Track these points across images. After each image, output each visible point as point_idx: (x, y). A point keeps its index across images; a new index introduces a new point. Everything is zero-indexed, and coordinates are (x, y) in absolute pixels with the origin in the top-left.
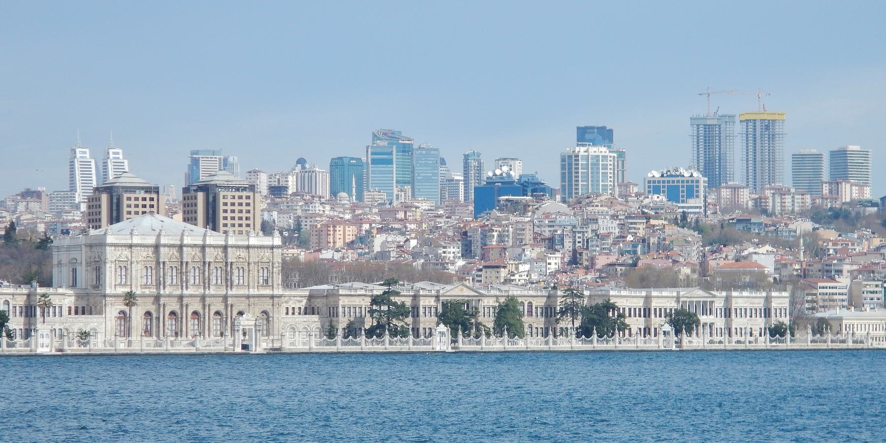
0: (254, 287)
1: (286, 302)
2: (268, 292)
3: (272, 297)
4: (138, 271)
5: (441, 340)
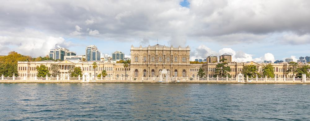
0: (180, 63)
2: (185, 64)
3: (187, 65)
4: (141, 58)
5: (240, 79)
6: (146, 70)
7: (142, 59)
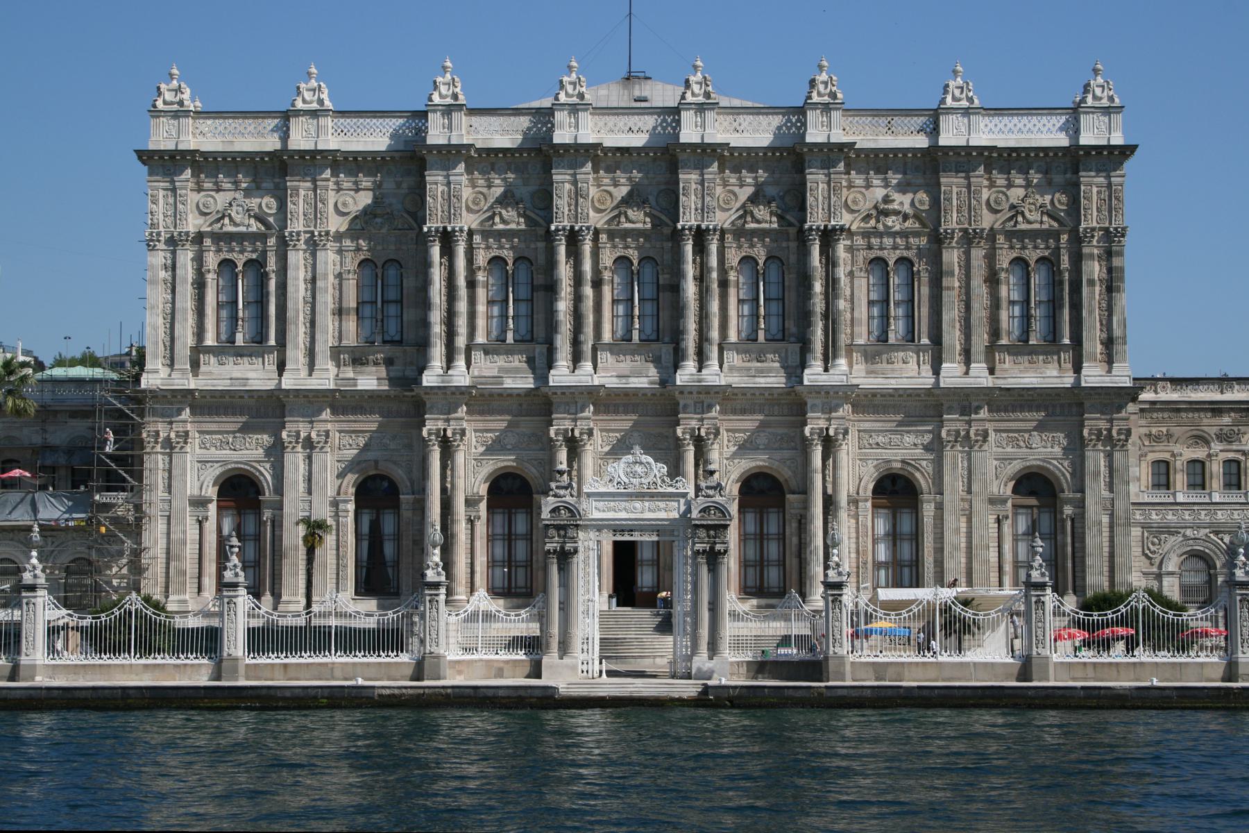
1: (1225, 438)
2: (1049, 375)
7: (327, 301)
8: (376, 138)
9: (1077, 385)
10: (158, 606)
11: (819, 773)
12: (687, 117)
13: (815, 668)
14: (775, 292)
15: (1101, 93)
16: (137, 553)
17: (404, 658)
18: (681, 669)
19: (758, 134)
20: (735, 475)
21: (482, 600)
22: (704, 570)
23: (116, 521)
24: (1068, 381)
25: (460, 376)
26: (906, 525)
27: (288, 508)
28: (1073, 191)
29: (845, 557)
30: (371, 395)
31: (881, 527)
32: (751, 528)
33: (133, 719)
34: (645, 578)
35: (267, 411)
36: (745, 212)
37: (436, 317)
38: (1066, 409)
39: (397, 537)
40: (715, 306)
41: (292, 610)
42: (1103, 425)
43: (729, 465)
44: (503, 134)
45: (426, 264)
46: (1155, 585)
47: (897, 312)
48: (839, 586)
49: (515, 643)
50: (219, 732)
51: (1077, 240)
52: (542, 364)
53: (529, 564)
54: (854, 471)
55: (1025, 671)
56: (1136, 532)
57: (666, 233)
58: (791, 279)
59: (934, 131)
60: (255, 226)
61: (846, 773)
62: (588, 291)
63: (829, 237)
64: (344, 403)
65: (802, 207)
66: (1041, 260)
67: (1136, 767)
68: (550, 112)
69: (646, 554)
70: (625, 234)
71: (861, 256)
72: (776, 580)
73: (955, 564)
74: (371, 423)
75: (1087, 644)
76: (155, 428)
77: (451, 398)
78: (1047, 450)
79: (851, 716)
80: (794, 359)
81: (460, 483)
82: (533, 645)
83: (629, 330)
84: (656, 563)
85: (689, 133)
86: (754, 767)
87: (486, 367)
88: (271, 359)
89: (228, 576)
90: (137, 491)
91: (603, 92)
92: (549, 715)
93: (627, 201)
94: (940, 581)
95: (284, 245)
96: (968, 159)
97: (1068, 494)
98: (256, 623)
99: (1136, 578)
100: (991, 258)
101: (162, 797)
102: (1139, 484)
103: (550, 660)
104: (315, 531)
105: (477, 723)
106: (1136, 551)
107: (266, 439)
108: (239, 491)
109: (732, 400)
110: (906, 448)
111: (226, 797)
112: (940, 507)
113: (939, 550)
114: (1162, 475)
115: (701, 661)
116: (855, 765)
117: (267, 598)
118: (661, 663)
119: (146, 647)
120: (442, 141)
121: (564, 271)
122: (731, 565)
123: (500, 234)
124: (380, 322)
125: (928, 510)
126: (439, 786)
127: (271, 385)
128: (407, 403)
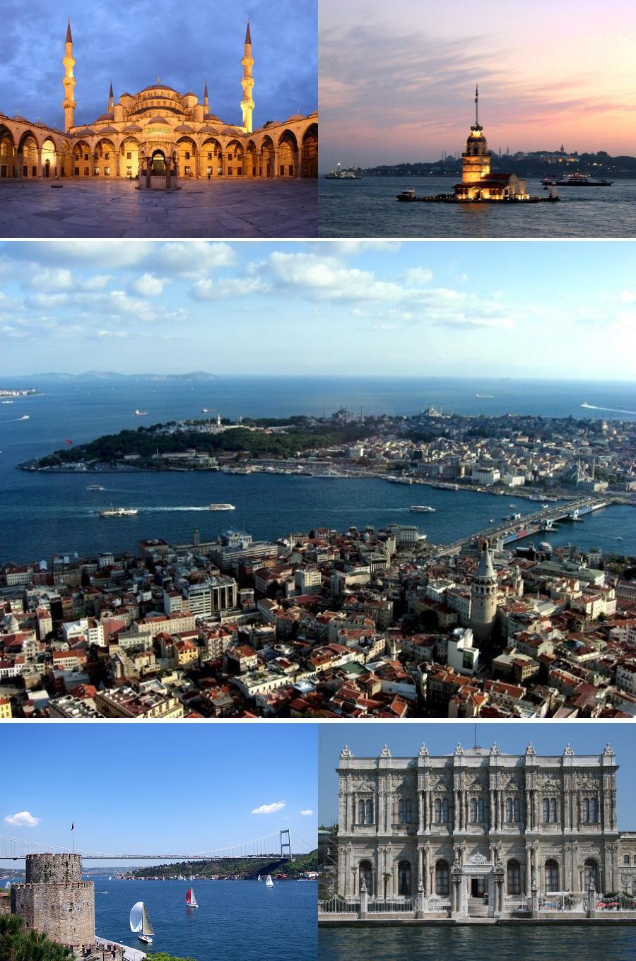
2: (595, 831)
6: (409, 865)
7: (390, 811)
8: (403, 765)
9: (603, 834)
10: (343, 898)
11: (529, 944)
12: (492, 758)
13: (529, 915)
14: (517, 808)
15: (609, 751)
16: (336, 883)
17: (412, 912)
18: (491, 915)
19: (512, 763)
20: (506, 860)
21: (434, 896)
22: (497, 887)
23: (331, 874)
24: (600, 833)
25: (428, 832)
26: (554, 874)
27: (379, 870)
28: (601, 779)
29: (537, 883)
30: (403, 838)
31: (547, 874)
32: (510, 875)
33: (335, 930)
34: (481, 889)
35: (373, 843)
36: (508, 786)
37: (421, 816)
38: (600, 841)
39: (410, 878)
40: (500, 812)
41: (380, 899)
42: (610, 845)
43: (504, 857)
44: (439, 764)
45: (418, 801)
46: (625, 890)
47: (551, 814)
48: (535, 891)
49: (444, 908)
50: (360, 933)
51: (603, 793)
52: (451, 829)
53: (448, 886)
54: (540, 859)
55: (589, 915)
56: (620, 875)
57: (486, 792)
58: (521, 805)
59: (562, 762)
60: (369, 790)
61: (538, 944)
62: (464, 808)
63: (532, 792)
64: (395, 840)
65: (525, 784)
66: (592, 799)
67: (620, 942)
68: (453, 757)
69: (480, 883)
70: (474, 792)
71: (541, 798)
72: (518, 889)
73: (568, 885)
74: (402, 846)
75: (606, 907)
76: (341, 847)
77: (425, 838)
78: (594, 853)
79: (539, 928)
80: (522, 827)
81: (428, 863)
82: (449, 909)
83: (476, 819)
84: (484, 885)
85: (492, 763)
86: (512, 943)
87: (435, 830)
88: (374, 828)
89: (362, 889)
90: (336, 865)
91: (468, 752)
92: (454, 928)
93: (475, 783)
94: (564, 890)
95: (378, 796)
96: (571, 770)
97: (600, 865)
98: (370, 903)
99: (620, 889)
100: (578, 798)
101: (344, 952)
102: (620, 862)
103: (454, 913)
104: (387, 876)
105: (433, 931)
106: (620, 881)
107: (373, 850)
108: (365, 865)
109: (505, 839)
110: (554, 852)
111: (362, 952)
112: (564, 869)
113: (564, 881)
114: (627, 859)
115: (497, 913)
116: (540, 942)
117: (373, 896)
118: (485, 913)
119: (339, 910)
120: (422, 766)
121: (457, 802)
122: (505, 885)
123: (439, 792)
124: (405, 817)
125: (561, 870)
126: (423, 949)
127: (374, 835)
128: (413, 840)
